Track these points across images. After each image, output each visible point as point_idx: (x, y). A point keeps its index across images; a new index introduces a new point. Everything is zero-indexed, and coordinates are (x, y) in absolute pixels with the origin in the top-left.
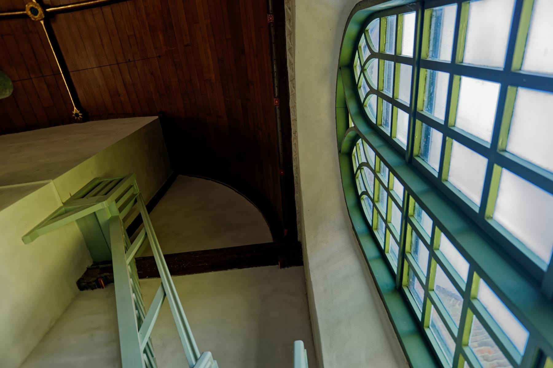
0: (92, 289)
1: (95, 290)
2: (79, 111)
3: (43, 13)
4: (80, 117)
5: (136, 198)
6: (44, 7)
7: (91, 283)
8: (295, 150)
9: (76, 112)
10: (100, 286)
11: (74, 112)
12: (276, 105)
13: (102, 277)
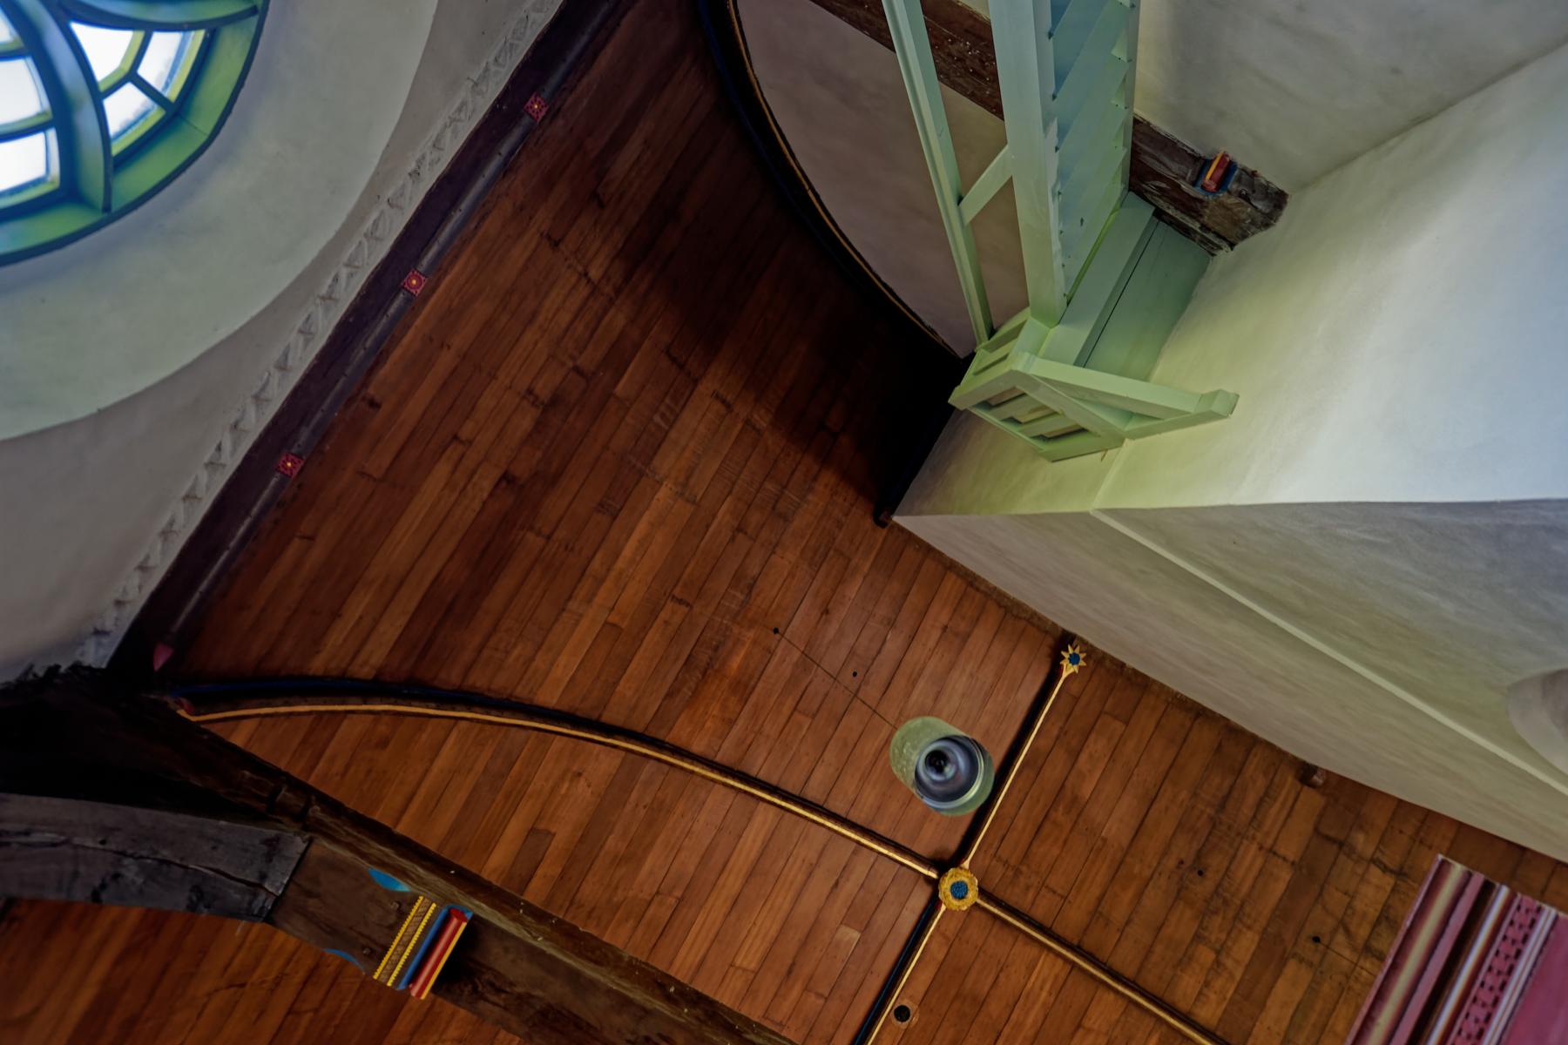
0: (1254, 174)
1: (1251, 167)
2: (1062, 663)
3: (946, 876)
4: (1077, 651)
5: (989, 339)
6: (934, 884)
7: (1240, 195)
8: (448, 133)
9: (1070, 665)
10: (1229, 167)
12: (423, 278)
13: (1203, 188)
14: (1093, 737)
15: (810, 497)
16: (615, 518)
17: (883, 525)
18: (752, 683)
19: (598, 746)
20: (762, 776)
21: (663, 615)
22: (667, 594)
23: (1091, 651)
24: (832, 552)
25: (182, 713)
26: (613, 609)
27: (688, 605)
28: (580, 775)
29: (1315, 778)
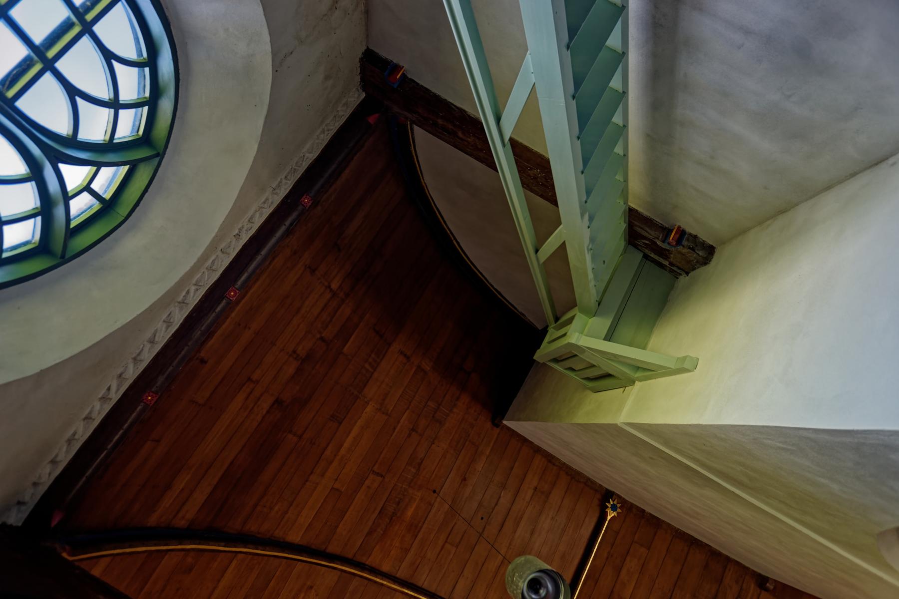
0: (696, 237)
1: (694, 233)
4: (615, 502)
5: (555, 323)
7: (689, 248)
8: (257, 215)
9: (612, 511)
10: (682, 233)
11: (614, 514)
12: (237, 291)
13: (669, 244)
14: (628, 559)
15: (455, 410)
16: (340, 423)
17: (497, 426)
18: (420, 525)
19: (324, 569)
20: (425, 586)
21: (367, 483)
22: (370, 470)
23: (624, 503)
24: (467, 443)
25: (65, 555)
26: (336, 480)
27: (382, 476)
28: (311, 587)
29: (768, 585)
